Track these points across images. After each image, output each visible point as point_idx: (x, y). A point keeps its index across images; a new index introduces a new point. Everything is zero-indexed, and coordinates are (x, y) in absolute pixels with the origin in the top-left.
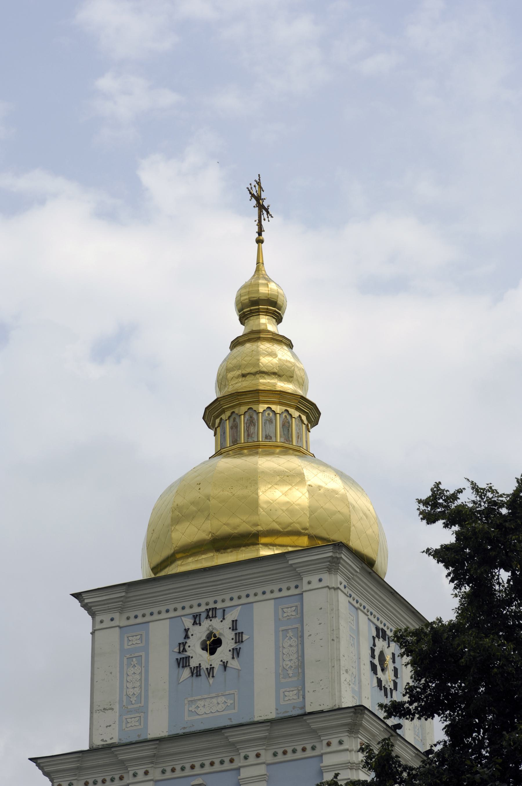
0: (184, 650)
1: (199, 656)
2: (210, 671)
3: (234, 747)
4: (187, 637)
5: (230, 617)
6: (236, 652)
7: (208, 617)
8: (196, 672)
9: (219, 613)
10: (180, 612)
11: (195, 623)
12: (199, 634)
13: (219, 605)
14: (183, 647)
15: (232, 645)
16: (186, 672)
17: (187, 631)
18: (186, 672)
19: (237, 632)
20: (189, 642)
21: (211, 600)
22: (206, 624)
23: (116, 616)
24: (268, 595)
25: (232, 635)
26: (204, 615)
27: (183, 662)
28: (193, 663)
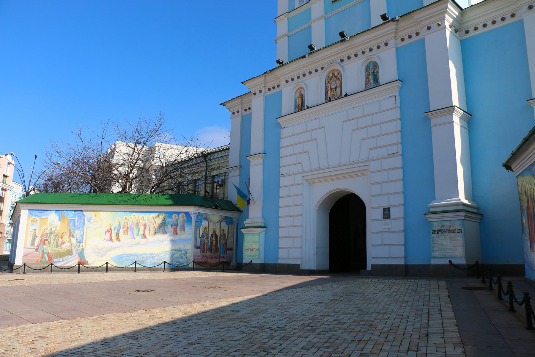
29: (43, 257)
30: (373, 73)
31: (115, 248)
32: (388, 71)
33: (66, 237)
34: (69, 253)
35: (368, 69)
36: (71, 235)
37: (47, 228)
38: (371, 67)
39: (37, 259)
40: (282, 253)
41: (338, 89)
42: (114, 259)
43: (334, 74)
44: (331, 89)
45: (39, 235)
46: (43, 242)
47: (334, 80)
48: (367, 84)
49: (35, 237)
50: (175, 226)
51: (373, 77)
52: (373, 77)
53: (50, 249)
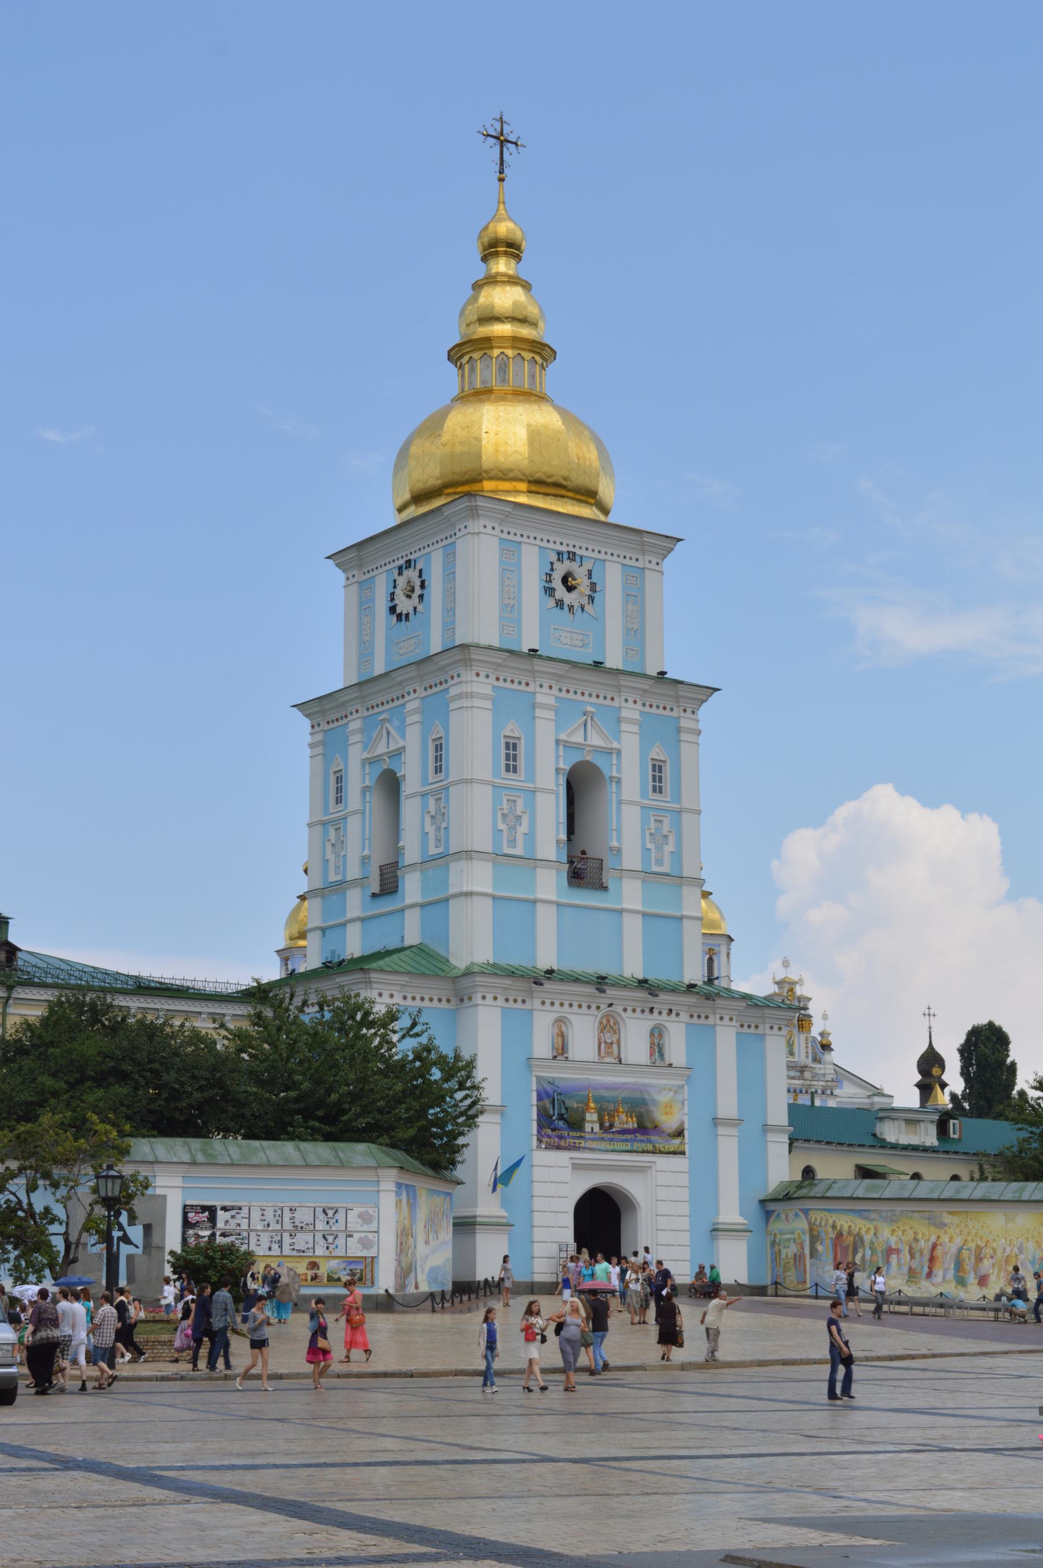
0: (550, 581)
1: (561, 591)
2: (571, 608)
4: (552, 569)
5: (588, 565)
7: (569, 558)
8: (560, 604)
9: (578, 558)
10: (544, 544)
11: (559, 560)
13: (577, 551)
14: (549, 577)
15: (588, 592)
17: (552, 564)
18: (551, 603)
19: (593, 581)
21: (571, 544)
23: (496, 525)
25: (587, 582)
26: (566, 556)
27: (550, 591)
30: (659, 1044)
32: (677, 1051)
35: (652, 1034)
38: (656, 1034)
41: (615, 1046)
43: (608, 1021)
44: (606, 1043)
47: (608, 1031)
48: (651, 1055)
51: (657, 1049)
52: (657, 1049)
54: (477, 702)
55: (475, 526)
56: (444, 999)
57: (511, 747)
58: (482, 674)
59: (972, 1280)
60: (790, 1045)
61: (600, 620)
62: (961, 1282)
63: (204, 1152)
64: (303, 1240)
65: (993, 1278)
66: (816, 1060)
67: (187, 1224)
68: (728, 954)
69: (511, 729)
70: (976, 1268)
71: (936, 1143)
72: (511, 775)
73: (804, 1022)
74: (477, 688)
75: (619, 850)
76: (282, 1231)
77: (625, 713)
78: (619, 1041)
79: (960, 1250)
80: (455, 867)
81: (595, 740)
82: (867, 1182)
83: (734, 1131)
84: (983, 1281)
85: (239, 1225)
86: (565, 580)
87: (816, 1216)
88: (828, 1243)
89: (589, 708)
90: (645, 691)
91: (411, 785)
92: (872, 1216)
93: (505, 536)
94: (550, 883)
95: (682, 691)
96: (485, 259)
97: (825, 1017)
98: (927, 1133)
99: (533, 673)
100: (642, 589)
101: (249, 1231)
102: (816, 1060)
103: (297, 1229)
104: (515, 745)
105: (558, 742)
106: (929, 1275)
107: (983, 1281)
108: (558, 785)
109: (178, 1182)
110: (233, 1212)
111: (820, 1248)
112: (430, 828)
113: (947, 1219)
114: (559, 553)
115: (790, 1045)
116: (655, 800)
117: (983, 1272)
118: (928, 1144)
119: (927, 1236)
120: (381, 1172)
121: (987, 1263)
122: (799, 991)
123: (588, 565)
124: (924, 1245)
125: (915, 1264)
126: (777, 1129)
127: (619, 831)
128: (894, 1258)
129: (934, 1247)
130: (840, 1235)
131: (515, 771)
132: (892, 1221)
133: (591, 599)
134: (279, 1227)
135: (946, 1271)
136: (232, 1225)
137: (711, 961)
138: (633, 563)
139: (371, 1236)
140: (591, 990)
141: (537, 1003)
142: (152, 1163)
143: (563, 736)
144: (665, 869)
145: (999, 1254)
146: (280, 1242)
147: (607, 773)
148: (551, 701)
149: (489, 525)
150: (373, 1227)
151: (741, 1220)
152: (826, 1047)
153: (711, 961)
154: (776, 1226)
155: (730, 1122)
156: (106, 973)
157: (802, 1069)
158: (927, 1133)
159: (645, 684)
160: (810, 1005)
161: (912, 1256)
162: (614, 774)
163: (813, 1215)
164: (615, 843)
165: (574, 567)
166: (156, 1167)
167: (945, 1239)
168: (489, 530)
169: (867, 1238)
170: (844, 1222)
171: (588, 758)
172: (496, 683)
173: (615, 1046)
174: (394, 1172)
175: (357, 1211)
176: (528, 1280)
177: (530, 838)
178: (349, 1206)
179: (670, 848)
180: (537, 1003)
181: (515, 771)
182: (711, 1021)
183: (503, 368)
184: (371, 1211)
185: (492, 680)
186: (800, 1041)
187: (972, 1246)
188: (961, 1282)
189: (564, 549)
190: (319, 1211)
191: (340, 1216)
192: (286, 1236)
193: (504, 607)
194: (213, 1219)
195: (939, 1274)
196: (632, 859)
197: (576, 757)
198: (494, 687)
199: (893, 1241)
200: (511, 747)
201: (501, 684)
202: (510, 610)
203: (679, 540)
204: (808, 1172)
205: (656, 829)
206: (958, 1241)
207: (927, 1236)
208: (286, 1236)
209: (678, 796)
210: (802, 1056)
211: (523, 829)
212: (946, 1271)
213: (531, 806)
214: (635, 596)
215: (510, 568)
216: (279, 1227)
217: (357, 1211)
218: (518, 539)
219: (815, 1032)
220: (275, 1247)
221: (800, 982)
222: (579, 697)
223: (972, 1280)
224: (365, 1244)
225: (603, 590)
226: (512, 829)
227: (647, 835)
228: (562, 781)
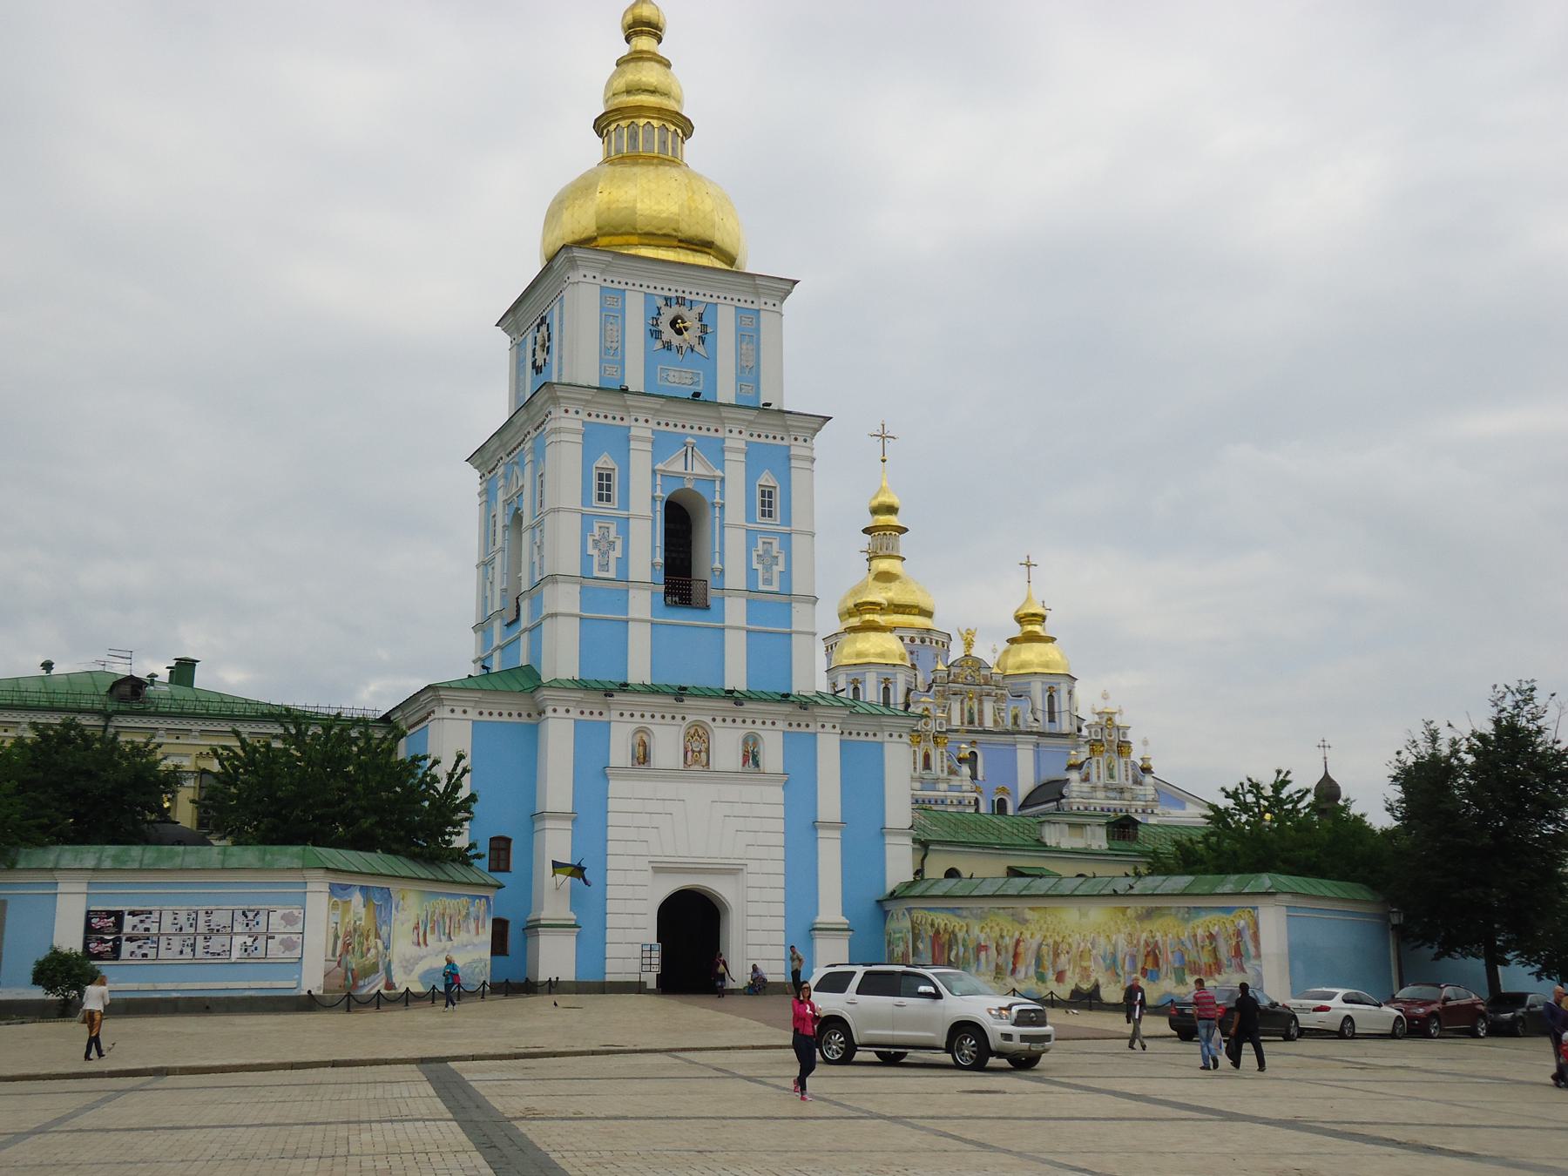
1: (668, 334)
2: (679, 348)
3: (722, 420)
6: (702, 340)
8: (668, 346)
10: (651, 291)
12: (668, 314)
13: (688, 296)
16: (659, 345)
18: (659, 345)
20: (662, 319)
22: (675, 310)
24: (728, 301)
27: (656, 334)
28: (665, 337)
29: (346, 978)
31: (422, 958)
33: (372, 938)
34: (374, 969)
35: (745, 742)
36: (378, 936)
37: (350, 917)
39: (340, 981)
40: (611, 966)
42: (423, 978)
45: (341, 934)
46: (346, 945)
49: (336, 937)
50: (477, 919)
51: (751, 757)
52: (751, 757)
53: (354, 962)
54: (564, 437)
55: (576, 276)
56: (524, 714)
57: (605, 478)
58: (572, 411)
59: (1051, 976)
60: (1110, 769)
61: (711, 359)
62: (1041, 978)
63: (115, 858)
64: (216, 943)
65: (1069, 974)
66: (1137, 782)
67: (89, 929)
68: (1070, 693)
69: (605, 461)
70: (1054, 964)
71: (1105, 846)
72: (604, 504)
73: (1123, 748)
74: (564, 423)
75: (722, 571)
76: (196, 935)
77: (728, 443)
78: (708, 750)
79: (1040, 946)
80: (547, 590)
81: (699, 469)
82: (1017, 880)
83: (837, 834)
84: (1060, 977)
85: (147, 929)
86: (673, 324)
87: (917, 914)
88: (928, 941)
89: (689, 440)
90: (751, 422)
91: (526, 522)
92: (965, 913)
93: (608, 284)
94: (643, 603)
95: (790, 420)
96: (628, 40)
97: (1145, 743)
98: (1094, 836)
99: (627, 408)
100: (758, 329)
101: (159, 935)
102: (1137, 782)
103: (212, 932)
104: (609, 477)
105: (654, 472)
106: (1014, 971)
107: (1060, 977)
108: (654, 511)
109: (83, 888)
110: (142, 917)
111: (921, 946)
112: (536, 558)
113: (1029, 915)
114: (666, 299)
115: (1110, 769)
116: (763, 524)
117: (1060, 968)
118: (1095, 847)
119: (1011, 931)
120: (308, 874)
121: (1063, 958)
122: (1118, 720)
123: (698, 309)
124: (1009, 942)
125: (1001, 961)
126: (898, 832)
127: (722, 554)
128: (983, 954)
129: (1018, 942)
130: (937, 932)
131: (608, 499)
132: (981, 918)
133: (702, 340)
134: (192, 930)
135: (1027, 967)
136: (140, 930)
137: (1051, 696)
138: (748, 305)
139: (294, 937)
140: (671, 701)
141: (615, 715)
142: (51, 870)
143: (659, 466)
144: (775, 588)
145: (1074, 950)
146: (193, 946)
147: (709, 500)
148: (649, 434)
149: (590, 274)
150: (298, 928)
151: (844, 920)
152: (1146, 770)
153: (1051, 696)
154: (892, 925)
155: (830, 825)
156: (258, 703)
157: (1121, 791)
158: (1094, 836)
159: (751, 415)
160: (1129, 732)
161: (999, 953)
162: (717, 499)
163: (915, 914)
164: (717, 565)
165: (683, 311)
166: (57, 874)
167: (1027, 935)
168: (589, 279)
169: (960, 935)
170: (941, 920)
171: (689, 486)
172: (587, 419)
173: (703, 755)
174: (321, 873)
175: (280, 912)
176: (600, 979)
177: (623, 562)
178: (272, 907)
179: (781, 567)
180: (615, 715)
181: (608, 499)
182: (811, 729)
183: (633, 137)
184: (296, 912)
185: (583, 416)
186: (1120, 765)
187: (1051, 941)
188: (1041, 978)
189: (672, 294)
190: (238, 915)
191: (262, 918)
192: (200, 939)
193: (605, 351)
194: (119, 924)
195: (1022, 969)
196: (735, 577)
197: (674, 487)
198: (584, 423)
199: (983, 937)
200: (605, 478)
201: (593, 419)
202: (612, 352)
203: (795, 282)
204: (952, 873)
205: (766, 551)
206: (1038, 937)
207: (1011, 931)
208: (200, 939)
209: (787, 520)
210: (1121, 779)
211: (617, 553)
212: (1027, 967)
213: (624, 531)
214: (749, 334)
215: (612, 312)
216: (192, 930)
217: (280, 912)
218: (623, 286)
219: (1136, 756)
220: (188, 950)
221: (1120, 712)
222: (679, 430)
223: (1051, 976)
224: (288, 945)
225: (715, 332)
226: (604, 554)
227: (755, 558)
228: (660, 507)
